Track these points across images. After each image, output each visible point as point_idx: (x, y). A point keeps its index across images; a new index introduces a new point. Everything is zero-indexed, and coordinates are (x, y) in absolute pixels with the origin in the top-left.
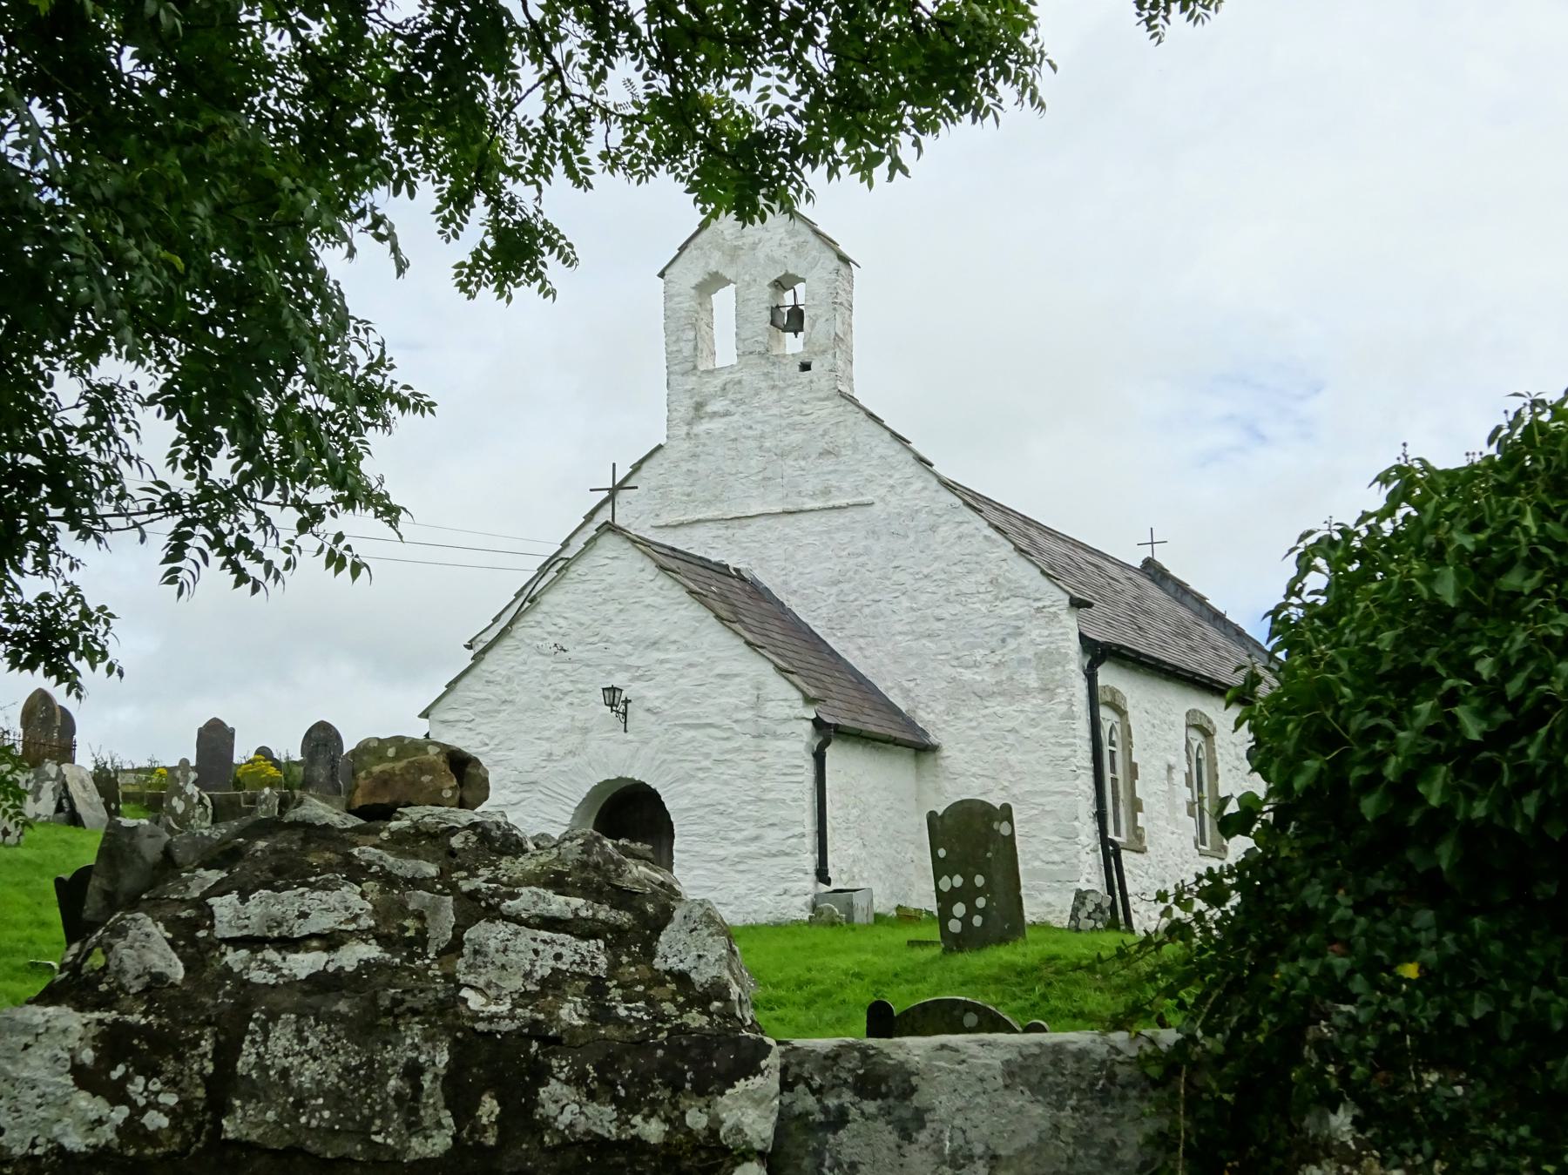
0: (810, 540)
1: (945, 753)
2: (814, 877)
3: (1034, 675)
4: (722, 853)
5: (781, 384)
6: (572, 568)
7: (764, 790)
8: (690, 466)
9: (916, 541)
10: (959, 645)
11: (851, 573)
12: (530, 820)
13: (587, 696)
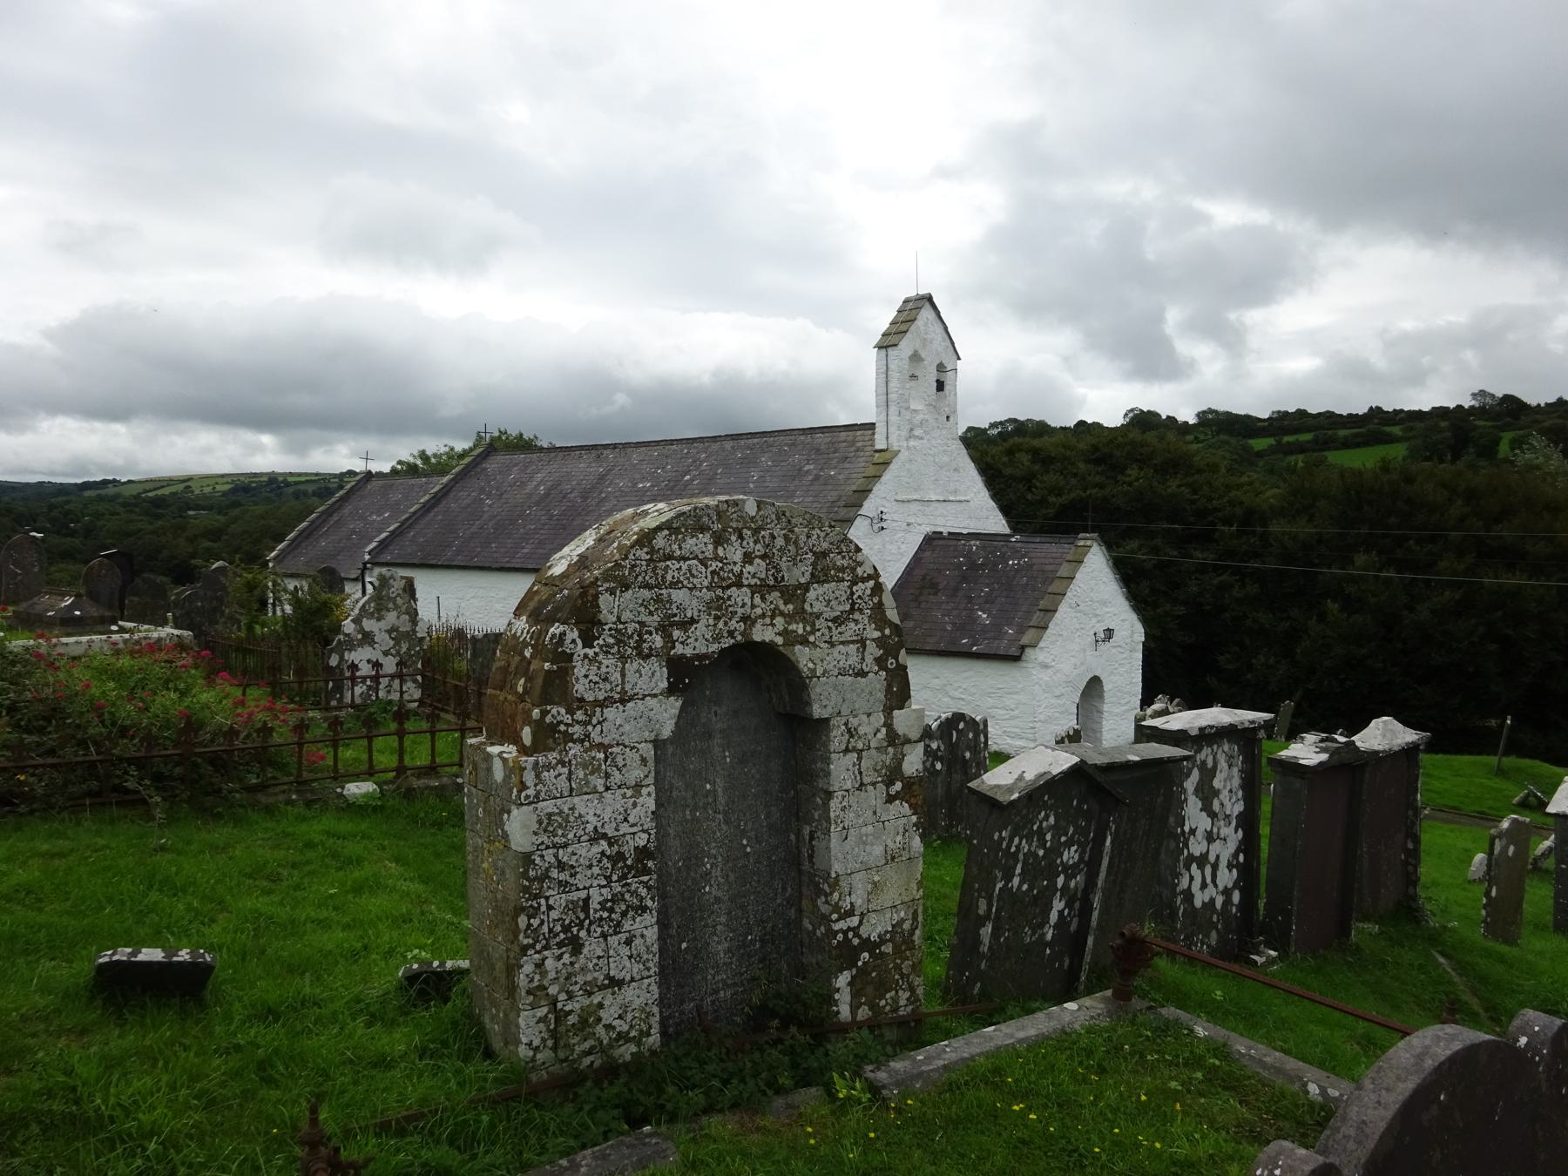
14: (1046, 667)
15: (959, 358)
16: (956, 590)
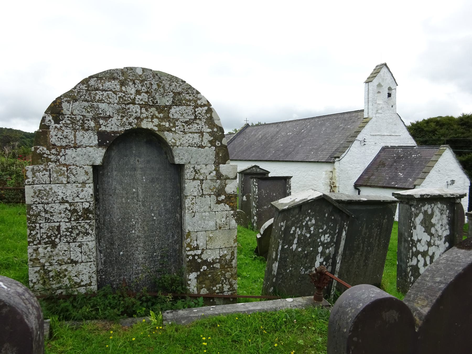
15: (397, 85)
16: (392, 165)
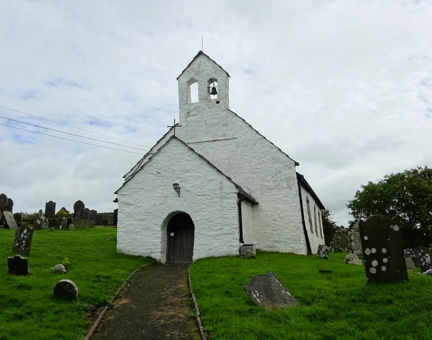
0: (220, 148)
1: (260, 205)
2: (239, 241)
3: (285, 183)
4: (210, 234)
5: (211, 107)
6: (162, 149)
7: (223, 214)
8: (186, 129)
9: (250, 148)
10: (263, 175)
11: (232, 156)
12: (149, 224)
13: (166, 187)
14: (129, 204)
